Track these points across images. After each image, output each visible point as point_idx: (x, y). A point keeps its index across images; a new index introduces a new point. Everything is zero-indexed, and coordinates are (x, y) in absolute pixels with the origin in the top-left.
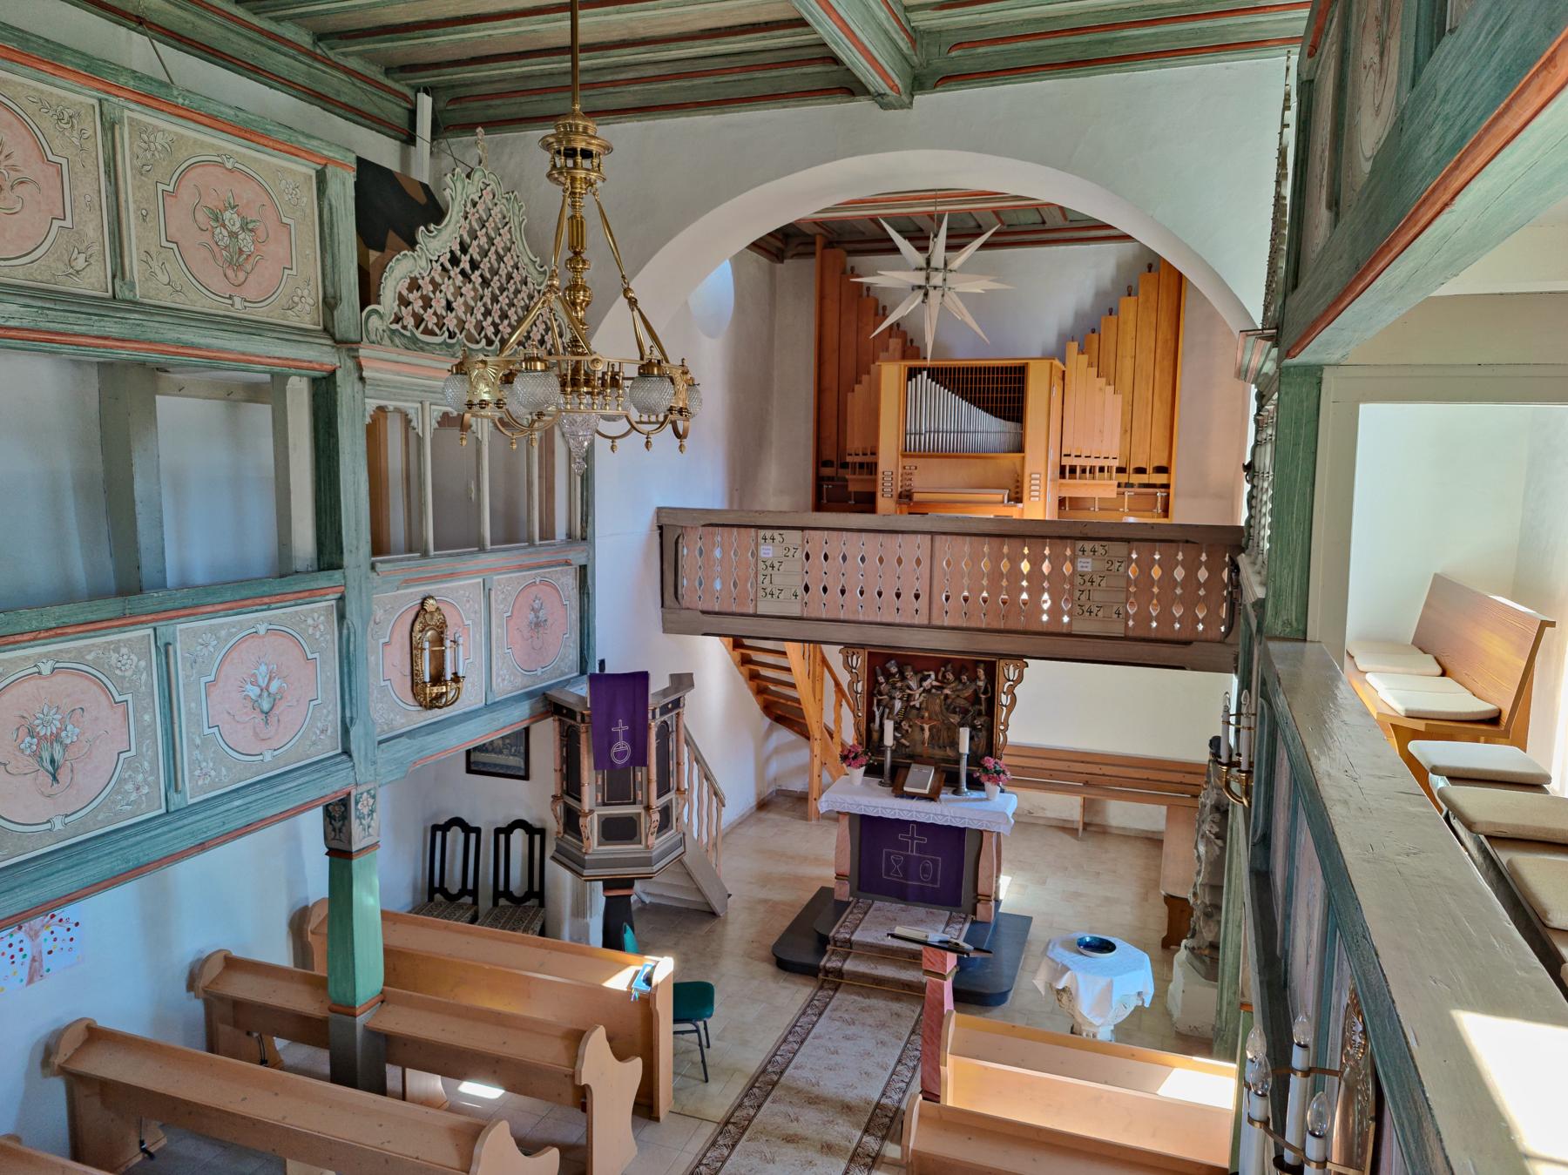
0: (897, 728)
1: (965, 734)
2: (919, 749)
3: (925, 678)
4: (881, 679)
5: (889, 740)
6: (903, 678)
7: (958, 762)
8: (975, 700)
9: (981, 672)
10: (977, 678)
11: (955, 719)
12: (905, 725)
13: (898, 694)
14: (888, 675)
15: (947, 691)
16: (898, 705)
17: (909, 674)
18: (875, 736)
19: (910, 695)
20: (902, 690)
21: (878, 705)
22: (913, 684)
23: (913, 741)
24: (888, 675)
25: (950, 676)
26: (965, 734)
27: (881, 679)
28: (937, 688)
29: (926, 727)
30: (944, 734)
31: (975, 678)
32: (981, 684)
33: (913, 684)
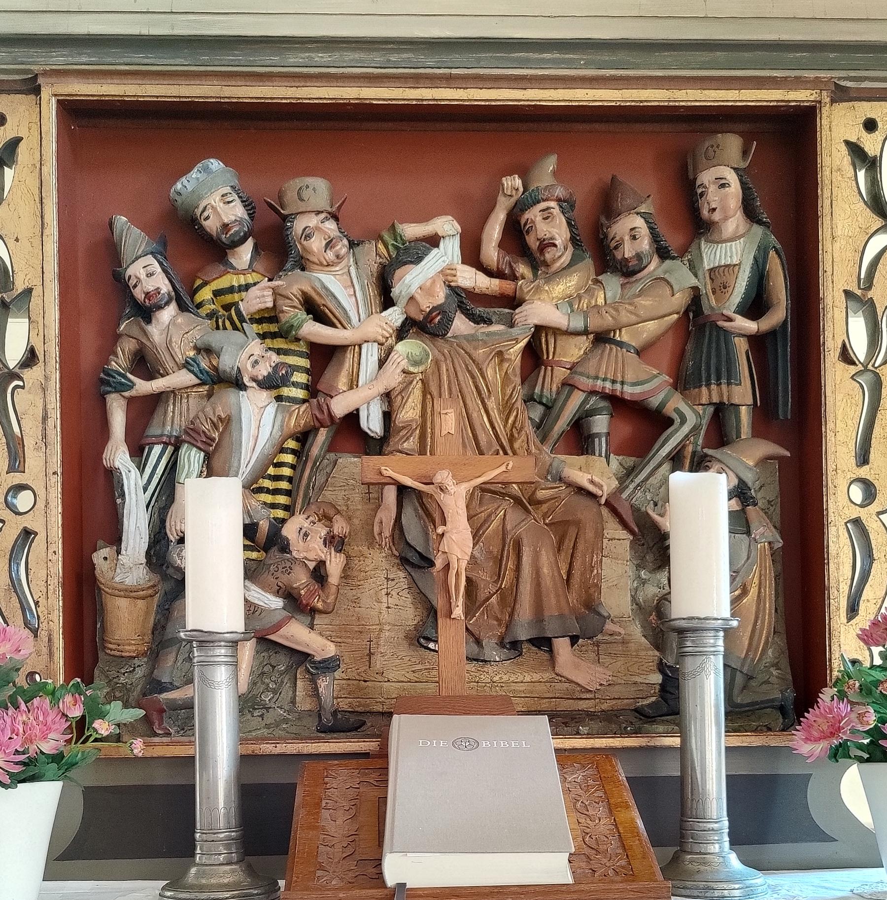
0: (263, 544)
1: (701, 507)
2: (395, 667)
3: (414, 252)
4: (148, 275)
5: (218, 593)
6: (278, 246)
7: (668, 704)
8: (696, 332)
9: (723, 185)
10: (699, 226)
11: (598, 473)
12: (305, 537)
13: (249, 354)
14: (194, 246)
15: (544, 307)
16: (259, 422)
17: (314, 230)
18: (126, 622)
19: (324, 356)
20: (272, 325)
21: (138, 451)
22: (342, 284)
23: (354, 632)
24: (194, 246)
25: (551, 227)
26: (701, 507)
27: (148, 275)
28: (464, 300)
29: (455, 500)
30: (541, 561)
31: (694, 223)
32: (735, 248)
33: (342, 284)
